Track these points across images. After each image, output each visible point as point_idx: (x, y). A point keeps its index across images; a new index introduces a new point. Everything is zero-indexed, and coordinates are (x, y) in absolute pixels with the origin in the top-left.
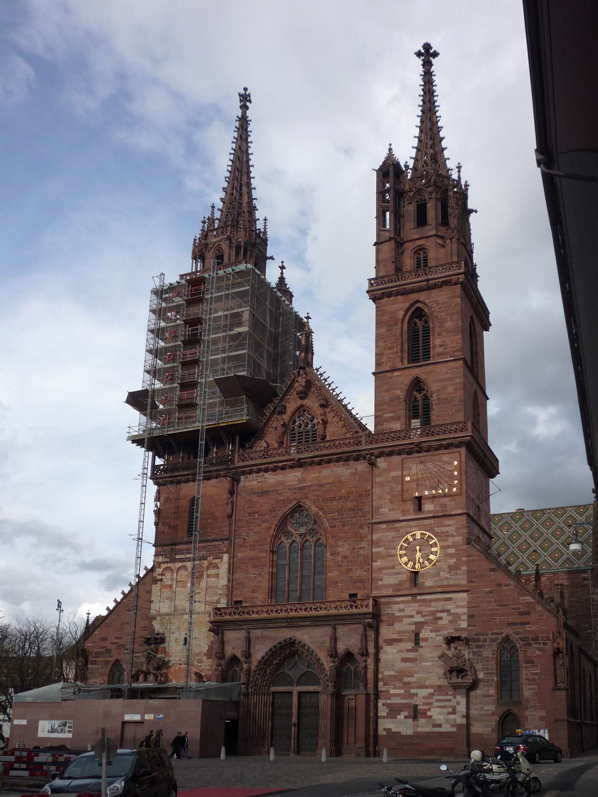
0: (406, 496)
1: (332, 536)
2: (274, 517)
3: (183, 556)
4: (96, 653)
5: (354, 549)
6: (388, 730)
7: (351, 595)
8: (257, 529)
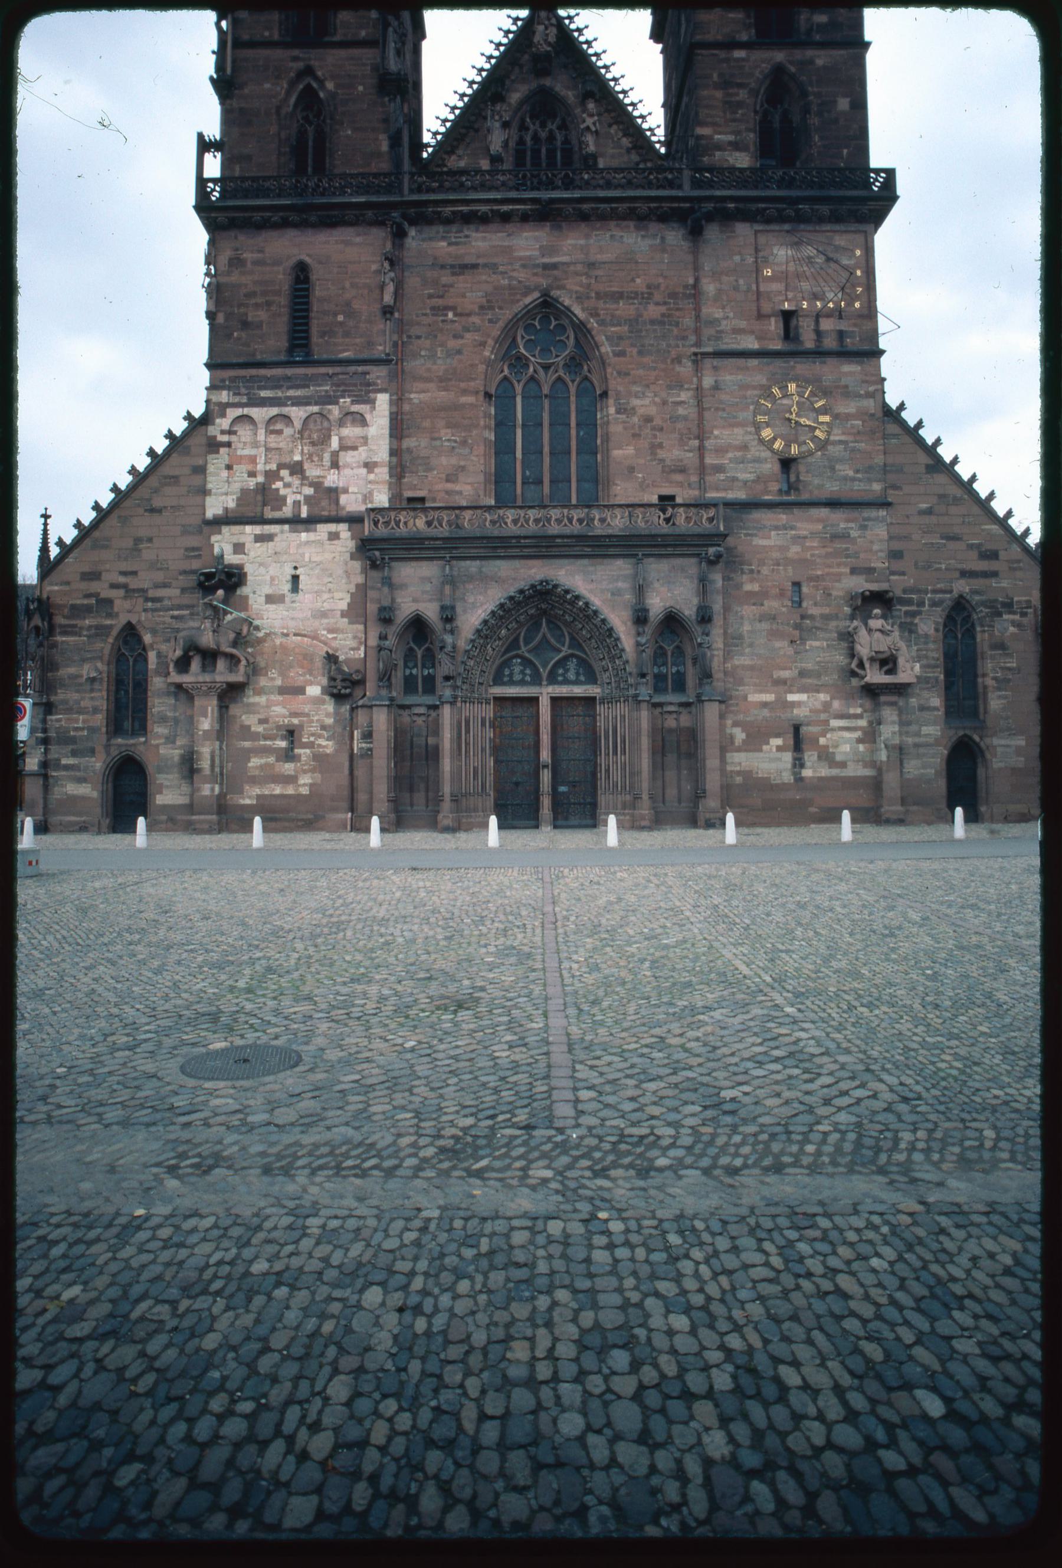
0: (767, 308)
1: (619, 373)
2: (490, 321)
3: (280, 394)
4: (73, 607)
5: (664, 403)
6: (747, 774)
7: (662, 498)
8: (452, 344)
